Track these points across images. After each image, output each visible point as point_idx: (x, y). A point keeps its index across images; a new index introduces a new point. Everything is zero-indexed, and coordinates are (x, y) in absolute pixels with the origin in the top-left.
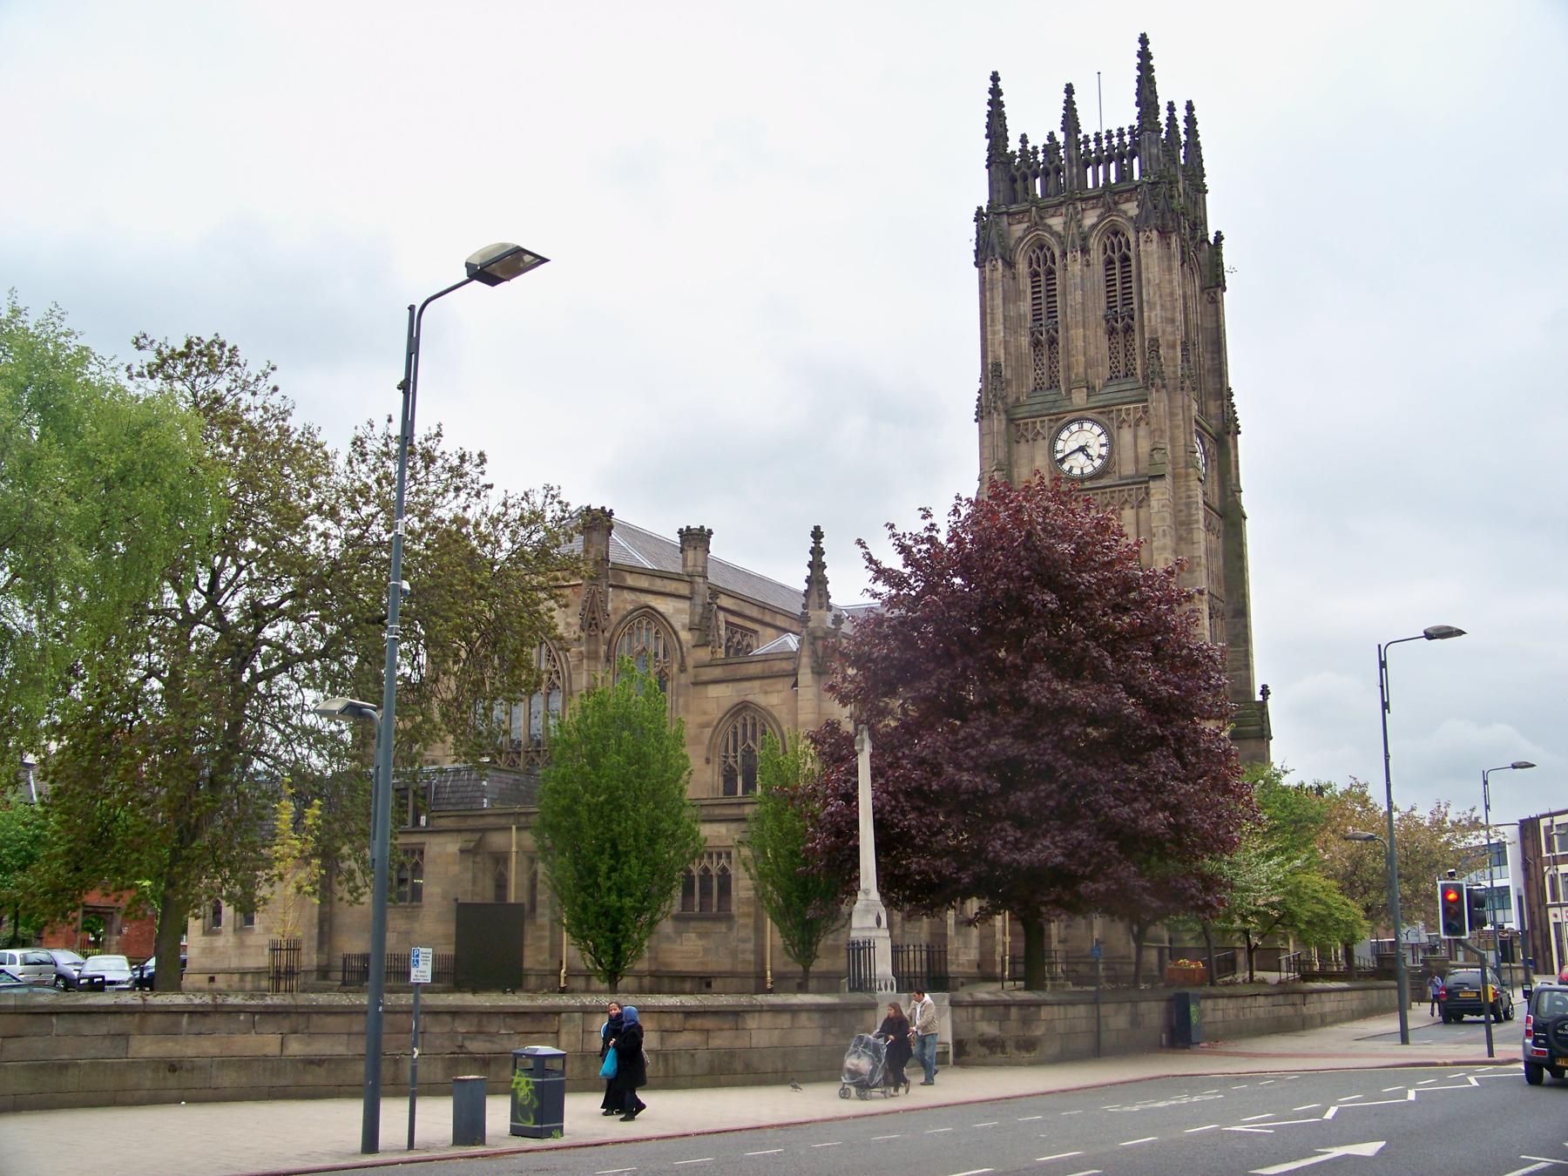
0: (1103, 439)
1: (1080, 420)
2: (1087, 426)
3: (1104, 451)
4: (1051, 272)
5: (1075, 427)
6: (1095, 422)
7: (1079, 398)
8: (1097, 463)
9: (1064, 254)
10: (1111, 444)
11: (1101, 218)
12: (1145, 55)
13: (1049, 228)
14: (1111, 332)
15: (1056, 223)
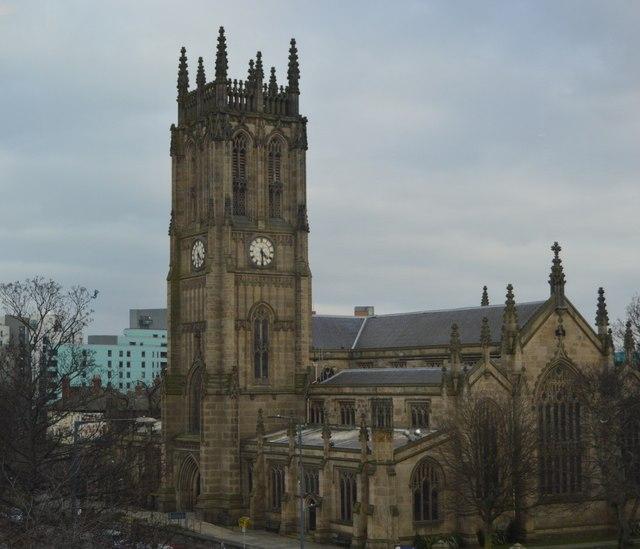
0: (272, 249)
1: (262, 237)
2: (265, 240)
3: (272, 255)
4: (243, 152)
5: (259, 240)
6: (269, 239)
7: (261, 225)
8: (269, 261)
9: (255, 146)
10: (275, 252)
11: (273, 131)
12: (293, 51)
13: (247, 129)
14: (271, 192)
15: (252, 127)
